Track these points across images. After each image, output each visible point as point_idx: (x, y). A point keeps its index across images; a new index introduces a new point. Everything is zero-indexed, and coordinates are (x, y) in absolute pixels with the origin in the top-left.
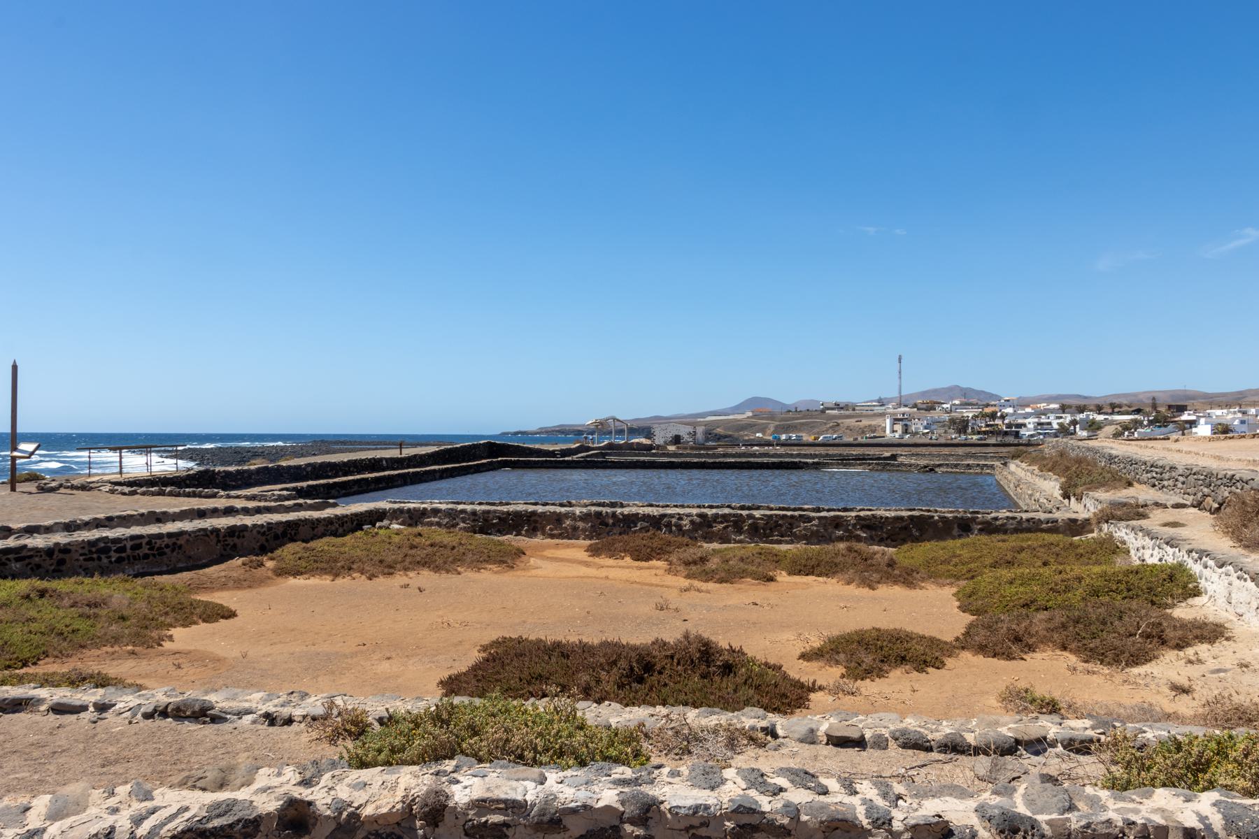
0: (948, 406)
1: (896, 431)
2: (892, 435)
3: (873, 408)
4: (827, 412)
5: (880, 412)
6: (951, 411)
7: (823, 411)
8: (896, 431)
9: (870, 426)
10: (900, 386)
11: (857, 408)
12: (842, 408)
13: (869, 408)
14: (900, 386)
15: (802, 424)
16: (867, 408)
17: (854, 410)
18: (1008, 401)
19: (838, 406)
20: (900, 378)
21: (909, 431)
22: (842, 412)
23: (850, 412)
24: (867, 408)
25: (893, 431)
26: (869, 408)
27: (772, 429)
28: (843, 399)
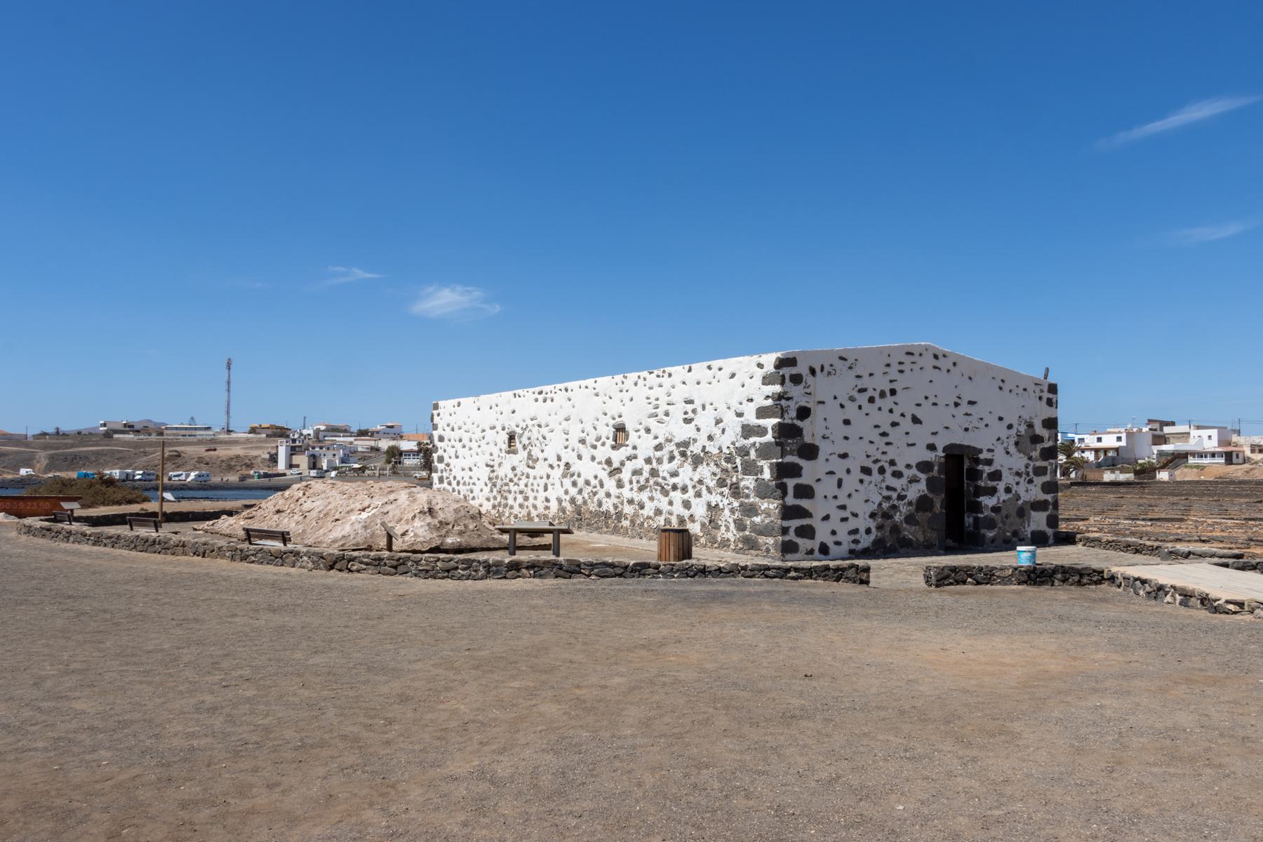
0: (311, 432)
1: (298, 466)
2: (295, 471)
3: (193, 432)
4: (116, 436)
5: (209, 438)
6: (318, 438)
7: (108, 435)
8: (298, 466)
9: (238, 457)
10: (229, 402)
11: (165, 432)
12: (138, 431)
13: (187, 432)
14: (229, 402)
15: (97, 453)
16: (183, 432)
17: (161, 434)
18: (392, 427)
19: (129, 428)
20: (228, 391)
21: (318, 466)
22: (142, 437)
23: (154, 437)
24: (183, 432)
25: (291, 466)
26: (187, 432)
27: (44, 462)
28: (136, 418)
